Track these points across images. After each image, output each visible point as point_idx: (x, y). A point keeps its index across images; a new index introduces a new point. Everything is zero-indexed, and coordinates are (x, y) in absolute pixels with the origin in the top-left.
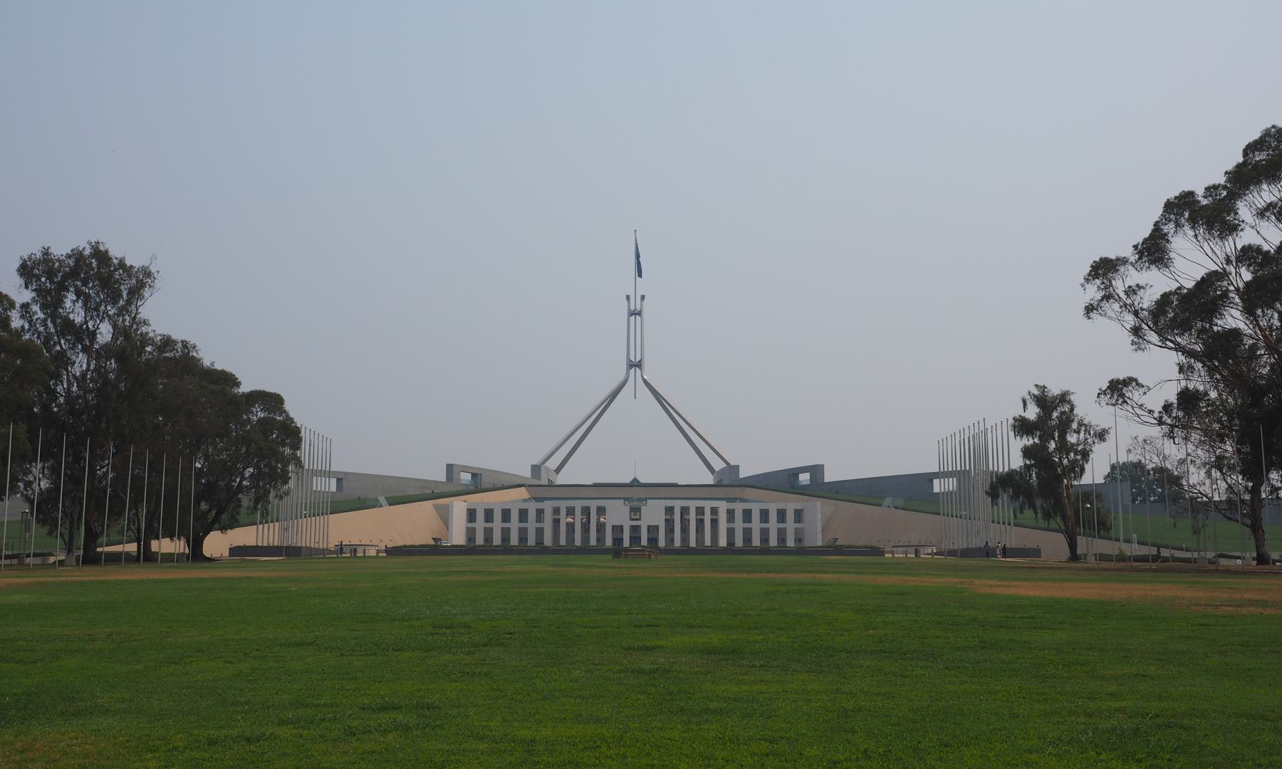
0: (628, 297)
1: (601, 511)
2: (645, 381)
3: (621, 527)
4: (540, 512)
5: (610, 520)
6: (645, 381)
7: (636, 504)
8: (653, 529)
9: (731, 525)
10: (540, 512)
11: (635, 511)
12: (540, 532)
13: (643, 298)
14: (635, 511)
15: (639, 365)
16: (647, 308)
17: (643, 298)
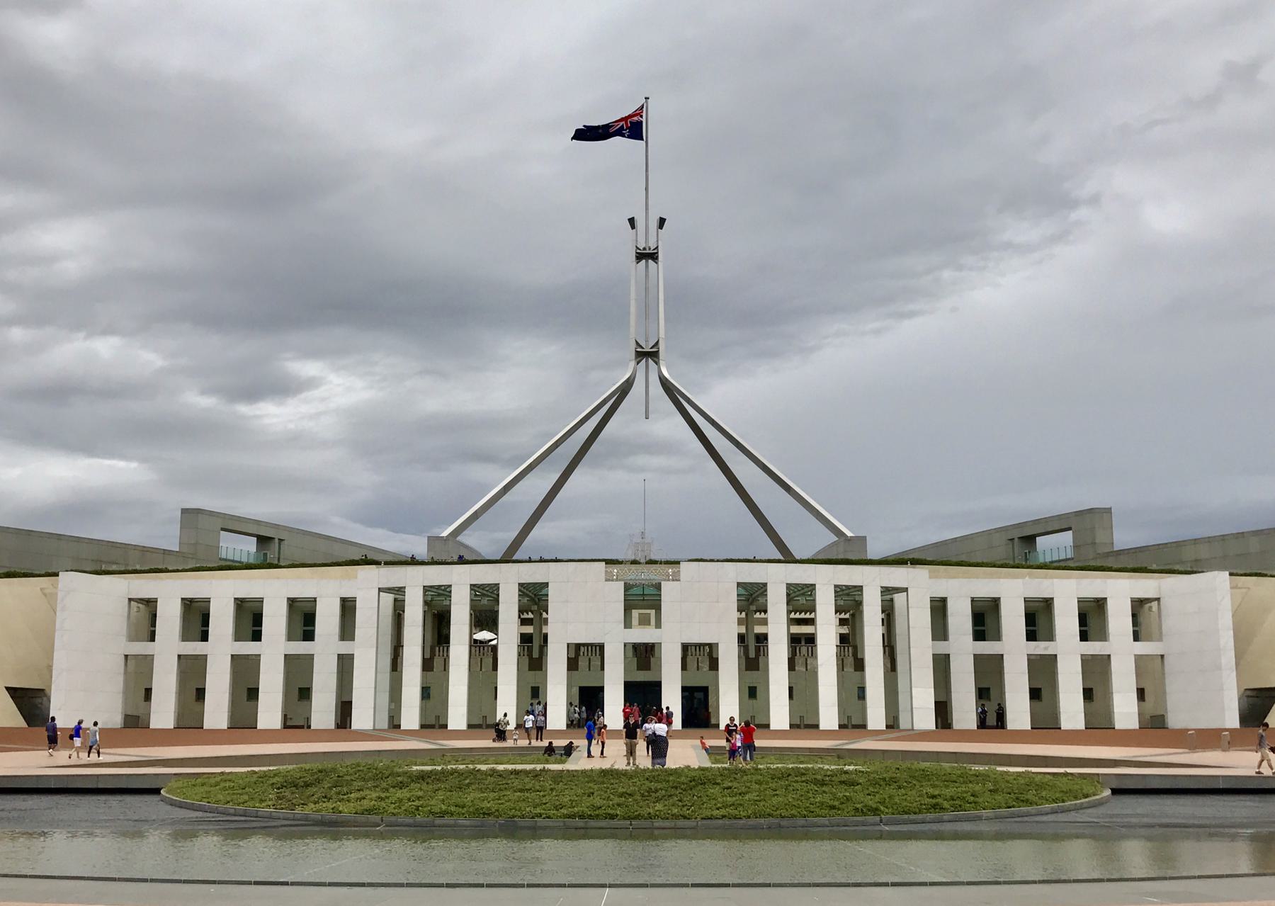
0: (632, 222)
1: (534, 600)
2: (665, 384)
3: (598, 649)
4: (348, 607)
5: (562, 631)
6: (665, 384)
7: (645, 574)
8: (700, 656)
9: (942, 647)
10: (348, 607)
11: (642, 601)
12: (345, 664)
13: (662, 222)
14: (642, 601)
15: (653, 355)
16: (665, 242)
17: (662, 222)
